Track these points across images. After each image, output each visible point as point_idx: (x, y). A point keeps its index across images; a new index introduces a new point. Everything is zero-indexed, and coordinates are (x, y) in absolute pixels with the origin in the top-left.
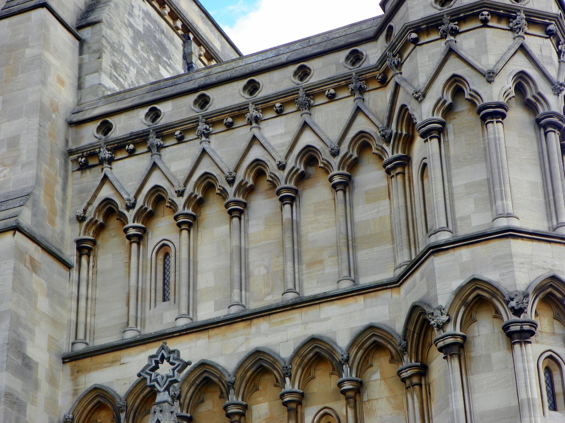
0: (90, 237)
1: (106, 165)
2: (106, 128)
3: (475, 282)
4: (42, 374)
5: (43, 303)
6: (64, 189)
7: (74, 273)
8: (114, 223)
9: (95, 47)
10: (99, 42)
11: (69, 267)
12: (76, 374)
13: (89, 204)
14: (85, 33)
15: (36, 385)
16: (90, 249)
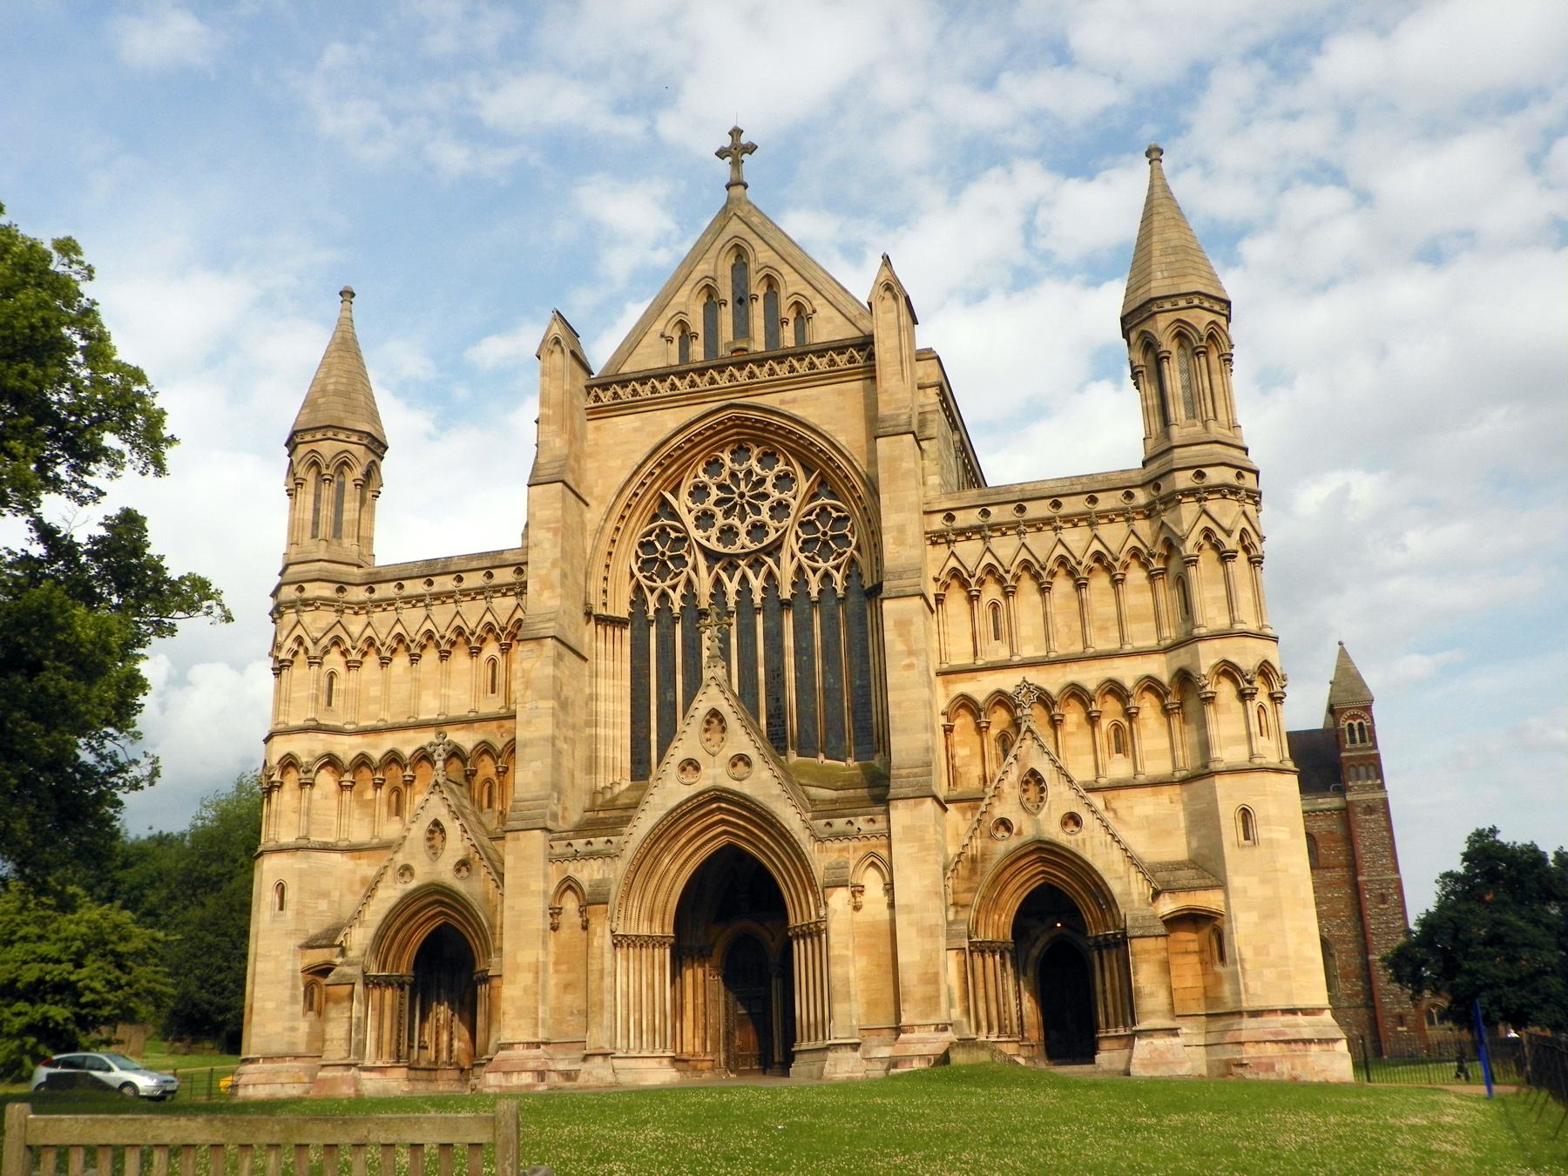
2: (950, 518)
3: (1226, 662)
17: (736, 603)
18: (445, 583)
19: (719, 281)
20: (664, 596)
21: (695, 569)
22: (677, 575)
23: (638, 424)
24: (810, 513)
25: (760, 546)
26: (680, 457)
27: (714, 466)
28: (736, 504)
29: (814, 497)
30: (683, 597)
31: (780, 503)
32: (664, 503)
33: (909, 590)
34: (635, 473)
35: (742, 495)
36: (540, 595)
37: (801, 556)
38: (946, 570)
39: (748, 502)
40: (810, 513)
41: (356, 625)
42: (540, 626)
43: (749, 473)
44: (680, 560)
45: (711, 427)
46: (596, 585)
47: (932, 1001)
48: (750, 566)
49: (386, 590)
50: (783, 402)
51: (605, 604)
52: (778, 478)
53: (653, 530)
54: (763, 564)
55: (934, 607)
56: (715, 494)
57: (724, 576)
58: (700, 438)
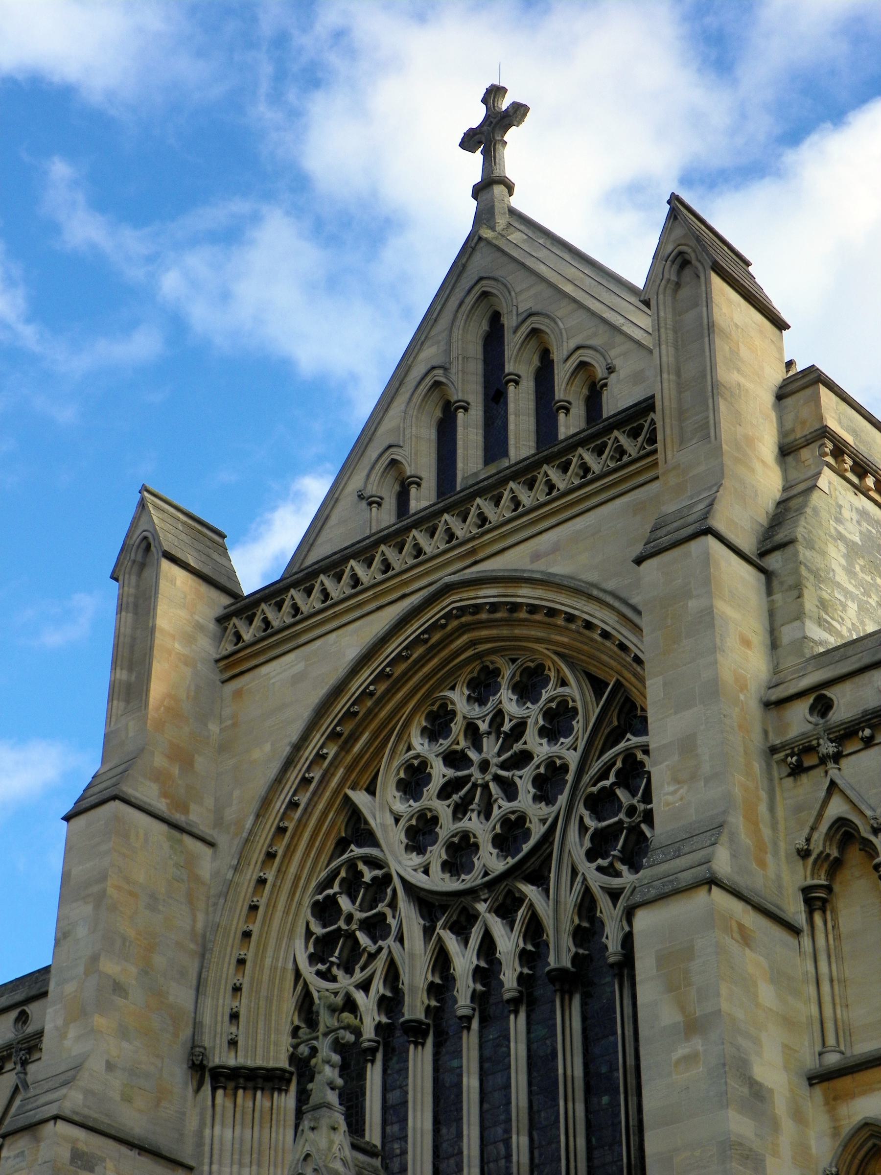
0: (823, 882)
1: (831, 765)
2: (823, 706)
4: (781, 1106)
5: (766, 994)
6: (772, 808)
7: (806, 941)
8: (854, 855)
9: (790, 581)
10: (796, 572)
11: (795, 931)
12: (832, 1102)
13: (813, 829)
14: (774, 562)
15: (775, 1126)
16: (824, 901)
17: (474, 996)
19: (453, 370)
21: (400, 939)
22: (372, 957)
23: (300, 667)
24: (604, 775)
25: (511, 861)
26: (371, 714)
28: (475, 786)
29: (615, 737)
30: (382, 1002)
31: (550, 763)
32: (355, 816)
33: (686, 877)
34: (289, 763)
35: (484, 766)
36: (63, 1036)
37: (588, 869)
38: (824, 827)
39: (497, 778)
40: (603, 775)
42: (43, 1099)
43: (499, 715)
45: (418, 641)
50: (536, 557)
51: (233, 1043)
52: (548, 714)
53: (335, 873)
54: (519, 900)
55: (801, 919)
56: (440, 772)
57: (452, 942)
58: (403, 666)
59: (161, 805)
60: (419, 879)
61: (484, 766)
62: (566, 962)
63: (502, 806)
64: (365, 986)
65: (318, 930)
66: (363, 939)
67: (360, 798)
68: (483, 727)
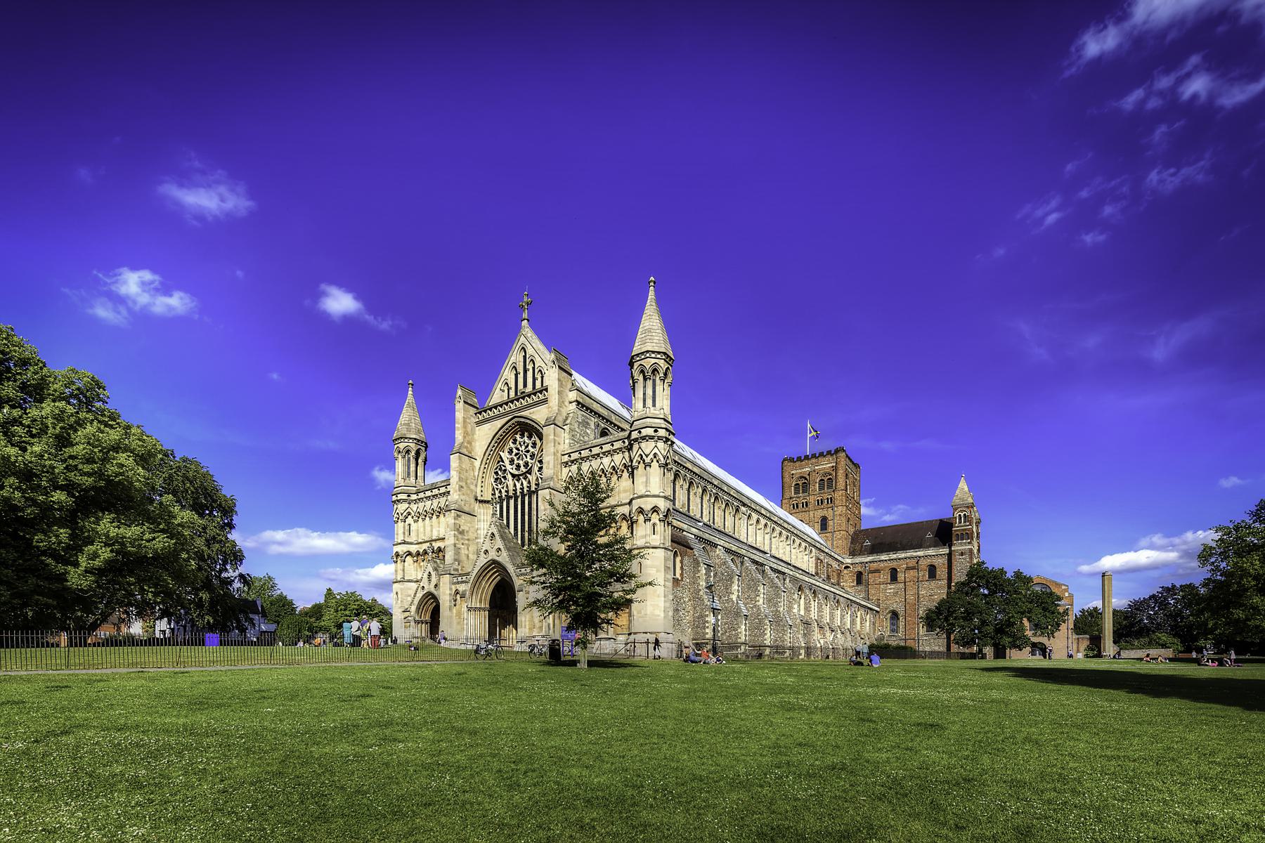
18: (436, 492)
20: (500, 492)
26: (503, 438)
27: (515, 441)
31: (532, 453)
32: (501, 457)
33: (546, 487)
34: (489, 446)
35: (522, 451)
41: (414, 507)
44: (504, 477)
46: (479, 489)
47: (541, 628)
48: (524, 479)
49: (421, 495)
56: (515, 451)
59: (466, 453)
60: (511, 471)
61: (522, 451)
62: (534, 489)
63: (525, 459)
64: (503, 488)
65: (495, 477)
66: (503, 479)
67: (501, 453)
68: (522, 444)
